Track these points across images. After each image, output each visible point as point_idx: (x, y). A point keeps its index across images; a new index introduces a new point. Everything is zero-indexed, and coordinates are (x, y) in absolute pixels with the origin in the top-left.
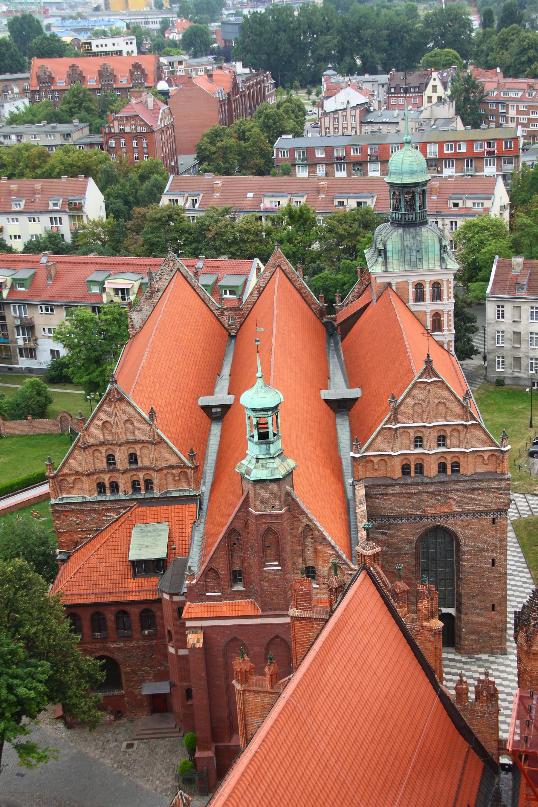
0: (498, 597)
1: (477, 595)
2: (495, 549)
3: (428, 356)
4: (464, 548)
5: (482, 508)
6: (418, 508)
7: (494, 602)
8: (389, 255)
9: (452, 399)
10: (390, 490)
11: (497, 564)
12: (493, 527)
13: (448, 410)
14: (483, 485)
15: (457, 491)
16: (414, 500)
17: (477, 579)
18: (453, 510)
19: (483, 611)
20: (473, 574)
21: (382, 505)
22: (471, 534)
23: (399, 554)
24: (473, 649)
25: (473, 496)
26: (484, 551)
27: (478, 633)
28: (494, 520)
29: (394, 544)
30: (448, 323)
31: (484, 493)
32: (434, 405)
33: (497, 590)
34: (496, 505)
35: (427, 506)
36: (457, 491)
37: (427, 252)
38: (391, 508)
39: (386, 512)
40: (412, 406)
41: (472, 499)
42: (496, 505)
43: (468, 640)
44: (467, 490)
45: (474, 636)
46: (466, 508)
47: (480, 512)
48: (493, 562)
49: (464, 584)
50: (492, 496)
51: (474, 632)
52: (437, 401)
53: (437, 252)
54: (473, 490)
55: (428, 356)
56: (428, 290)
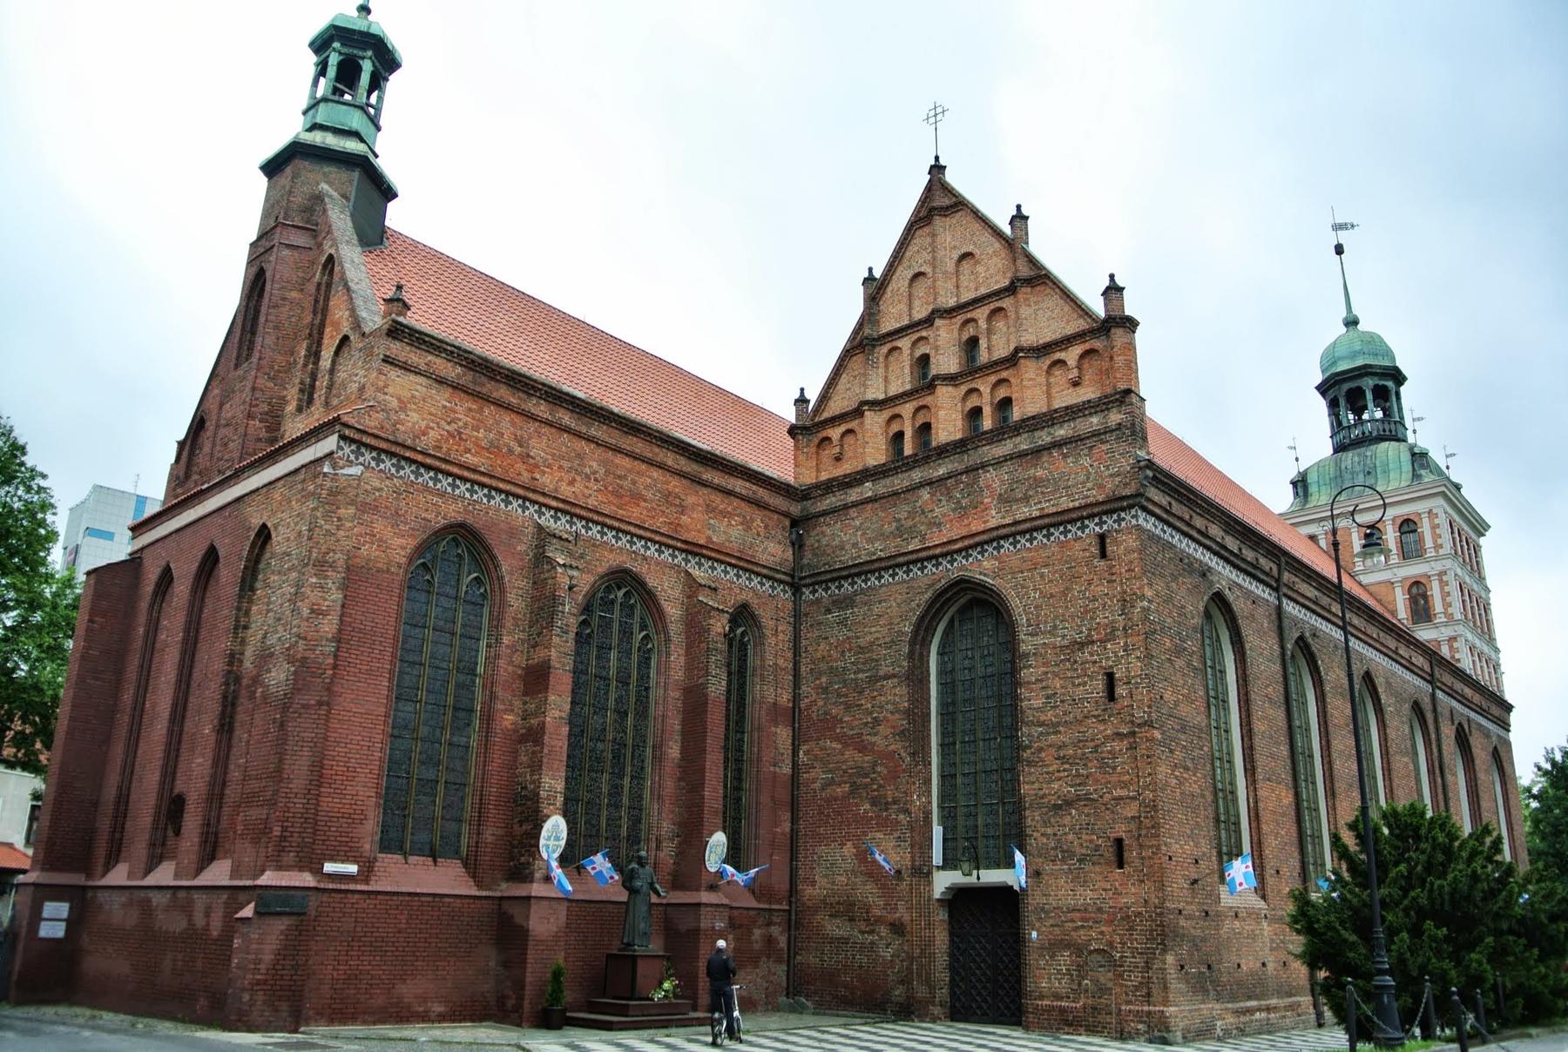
0: (1131, 810)
1: (1069, 803)
2: (1111, 637)
3: (937, 158)
4: (1027, 644)
5: (1066, 503)
6: (912, 532)
7: (1121, 830)
8: (1313, 489)
9: (987, 237)
10: (854, 495)
11: (1121, 690)
12: (1101, 564)
13: (980, 269)
14: (1061, 432)
15: (999, 463)
16: (902, 511)
17: (1063, 746)
18: (993, 523)
19: (1088, 867)
20: (1054, 727)
21: (837, 542)
22: (1043, 595)
23: (874, 680)
24: (1062, 1010)
25: (1040, 473)
26: (1082, 645)
27: (1078, 949)
28: (1102, 538)
29: (862, 650)
30: (1443, 600)
31: (1065, 456)
32: (950, 266)
33: (1125, 785)
34: (1101, 487)
35: (931, 524)
36: (999, 463)
37: (1386, 472)
38: (855, 545)
39: (847, 557)
40: (906, 283)
41: (1038, 482)
42: (1101, 487)
43: (1048, 977)
44: (1022, 455)
45: (1065, 959)
46: (1024, 512)
47: (1063, 519)
48: (1110, 677)
49: (1030, 763)
50: (1086, 461)
51: (1068, 946)
52: (956, 256)
53: (1407, 467)
54: (1037, 452)
55: (937, 158)
56: (1390, 536)
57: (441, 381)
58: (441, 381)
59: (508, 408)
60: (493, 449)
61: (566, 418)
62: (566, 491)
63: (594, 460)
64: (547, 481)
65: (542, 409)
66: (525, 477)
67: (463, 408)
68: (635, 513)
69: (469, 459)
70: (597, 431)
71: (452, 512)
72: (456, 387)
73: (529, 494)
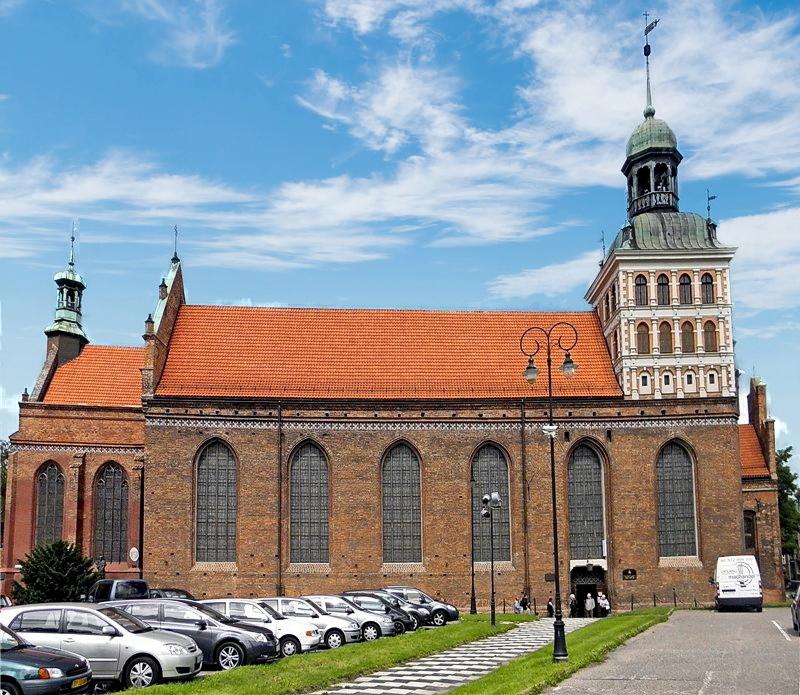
57: (37, 417)
58: (37, 417)
59: (61, 418)
60: (58, 433)
61: (83, 414)
62: (85, 439)
63: (94, 424)
64: (77, 438)
65: (74, 414)
66: (70, 439)
67: (46, 423)
68: (112, 440)
69: (50, 439)
70: (96, 415)
71: (47, 457)
72: (42, 417)
73: (73, 444)
